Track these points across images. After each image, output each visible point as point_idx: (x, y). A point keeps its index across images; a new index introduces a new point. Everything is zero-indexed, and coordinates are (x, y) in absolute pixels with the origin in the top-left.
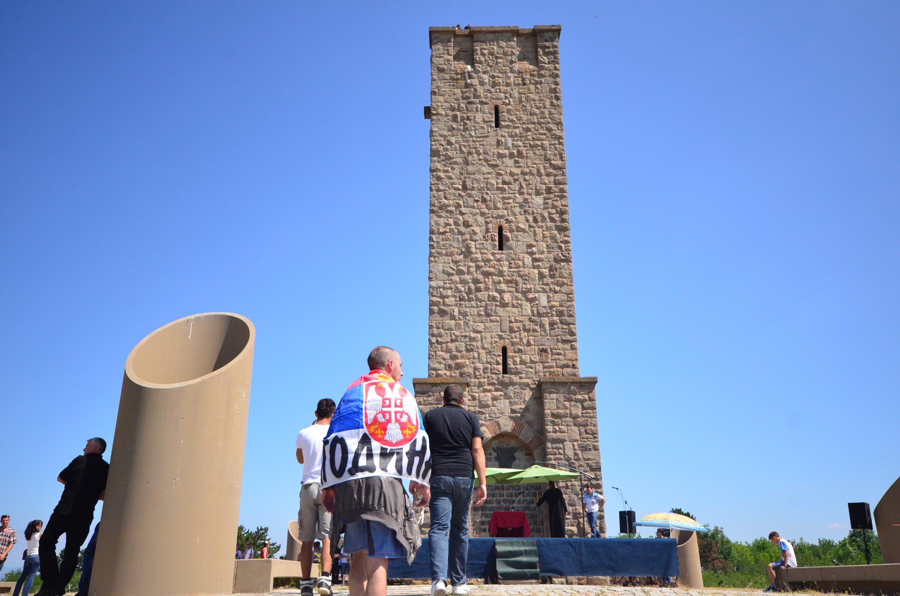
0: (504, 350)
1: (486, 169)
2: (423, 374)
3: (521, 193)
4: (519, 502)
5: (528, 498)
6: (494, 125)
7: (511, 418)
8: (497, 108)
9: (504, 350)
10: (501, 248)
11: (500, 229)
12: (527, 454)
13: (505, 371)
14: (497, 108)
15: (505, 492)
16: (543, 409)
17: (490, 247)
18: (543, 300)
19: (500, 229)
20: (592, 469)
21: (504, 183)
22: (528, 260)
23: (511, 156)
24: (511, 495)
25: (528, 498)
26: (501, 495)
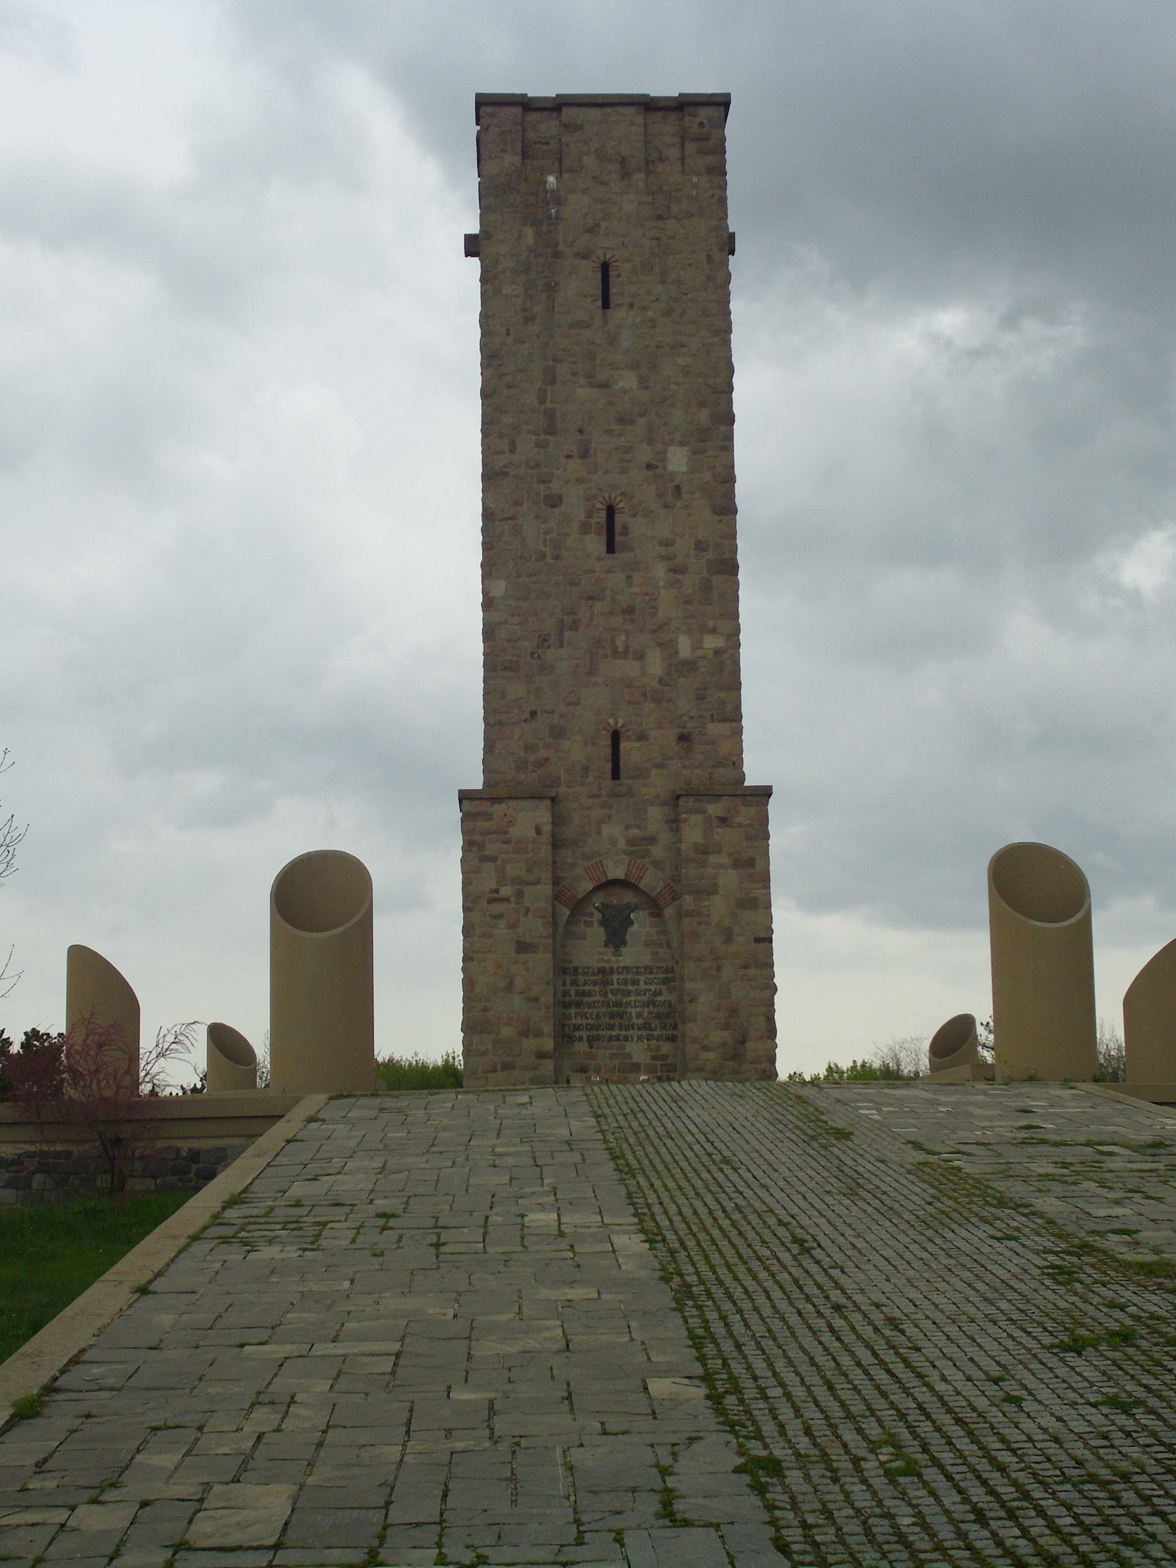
0: (616, 737)
1: (583, 392)
2: (476, 781)
3: (651, 442)
6: (600, 303)
7: (630, 854)
8: (605, 268)
9: (616, 737)
10: (611, 549)
11: (611, 511)
12: (652, 915)
13: (616, 775)
14: (605, 268)
16: (680, 841)
17: (595, 544)
18: (685, 646)
19: (611, 511)
20: (758, 940)
21: (621, 420)
22: (660, 571)
23: (635, 366)
24: (625, 982)
25: (653, 987)
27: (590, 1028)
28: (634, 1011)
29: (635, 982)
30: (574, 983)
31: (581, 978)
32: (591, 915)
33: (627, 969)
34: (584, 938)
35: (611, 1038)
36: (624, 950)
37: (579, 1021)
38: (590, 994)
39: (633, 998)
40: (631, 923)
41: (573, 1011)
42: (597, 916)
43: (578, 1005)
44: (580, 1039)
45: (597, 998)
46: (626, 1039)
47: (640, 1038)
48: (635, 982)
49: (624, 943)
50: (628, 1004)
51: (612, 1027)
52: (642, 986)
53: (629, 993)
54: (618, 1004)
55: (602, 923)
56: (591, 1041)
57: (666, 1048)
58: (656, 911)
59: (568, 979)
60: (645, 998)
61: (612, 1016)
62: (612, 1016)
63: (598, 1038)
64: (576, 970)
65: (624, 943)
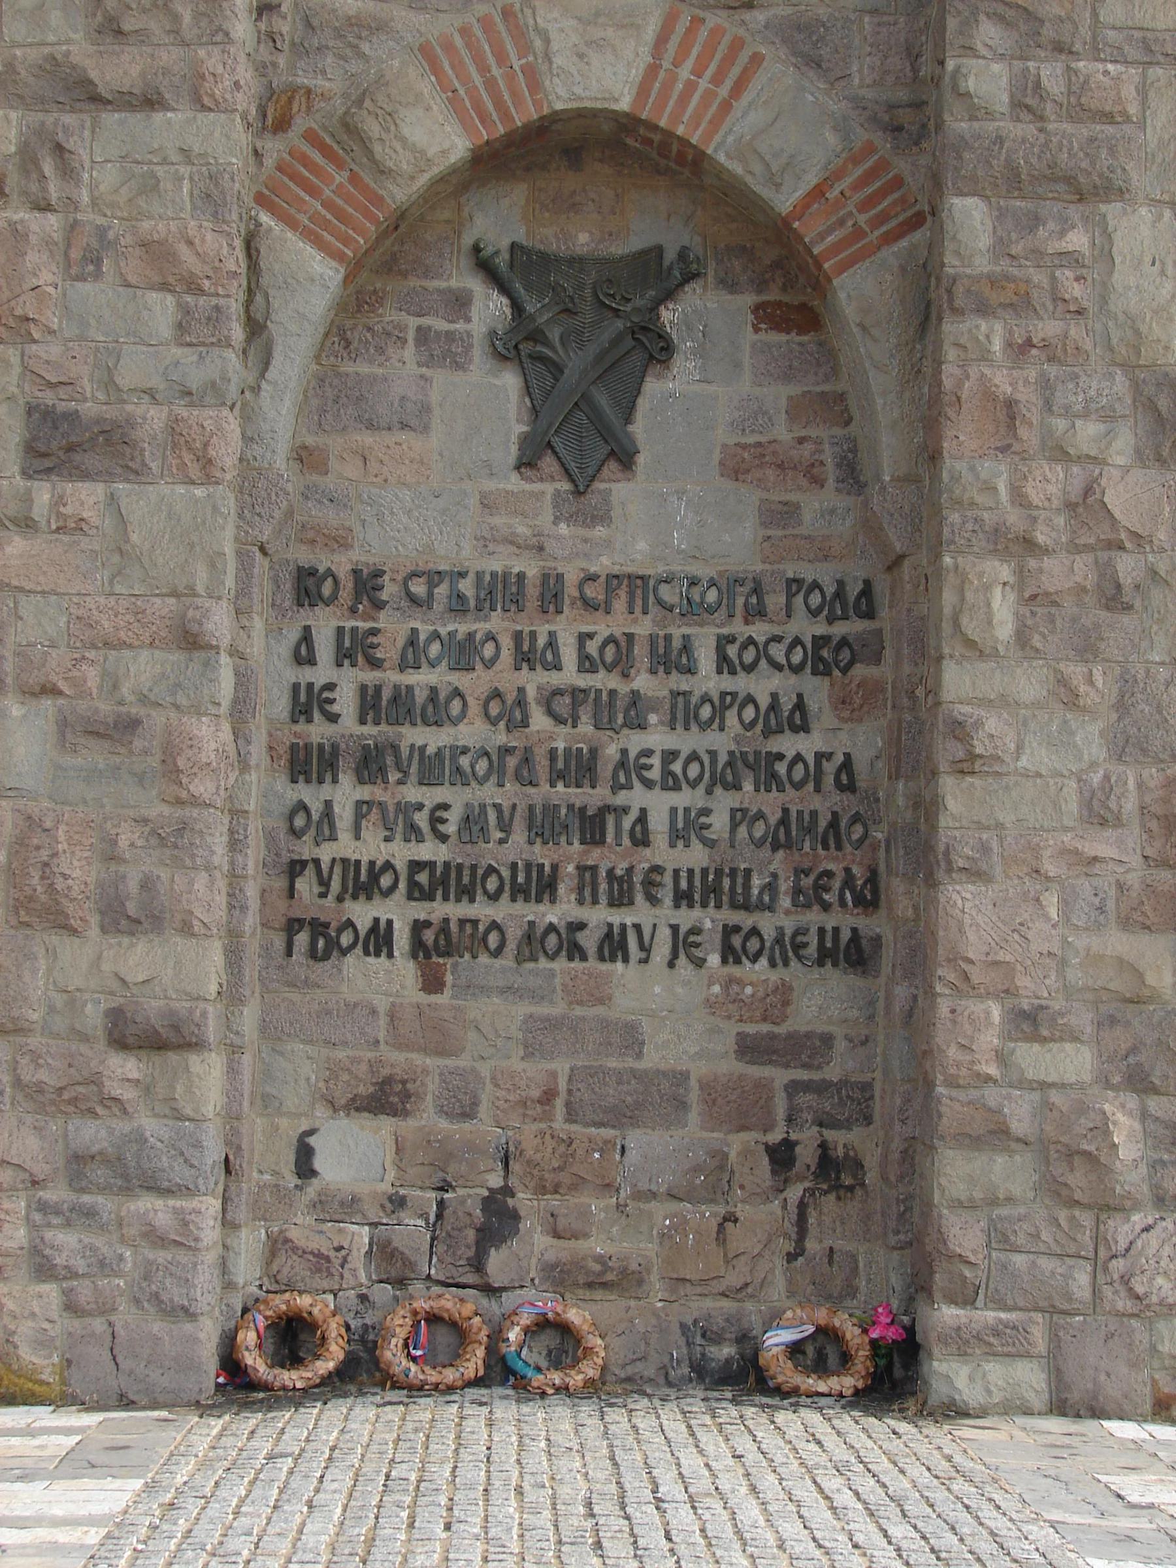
4: (683, 712)
5: (763, 685)
12: (770, 316)
15: (566, 629)
24: (620, 656)
25: (763, 685)
26: (526, 657)
27: (429, 882)
28: (659, 806)
29: (672, 659)
30: (355, 649)
31: (393, 628)
32: (460, 303)
33: (636, 587)
34: (414, 419)
35: (534, 942)
36: (620, 492)
37: (371, 847)
38: (435, 709)
39: (656, 737)
40: (657, 349)
41: (345, 793)
42: (489, 309)
43: (371, 764)
44: (379, 940)
45: (472, 732)
46: (614, 945)
47: (684, 944)
48: (672, 659)
49: (624, 457)
50: (630, 769)
51: (543, 886)
52: (707, 679)
53: (635, 713)
54: (580, 767)
55: (519, 345)
56: (434, 948)
57: (820, 1000)
58: (794, 302)
59: (325, 624)
60: (721, 742)
61: (545, 825)
62: (545, 825)
63: (478, 938)
64: (367, 585)
65: (624, 457)
